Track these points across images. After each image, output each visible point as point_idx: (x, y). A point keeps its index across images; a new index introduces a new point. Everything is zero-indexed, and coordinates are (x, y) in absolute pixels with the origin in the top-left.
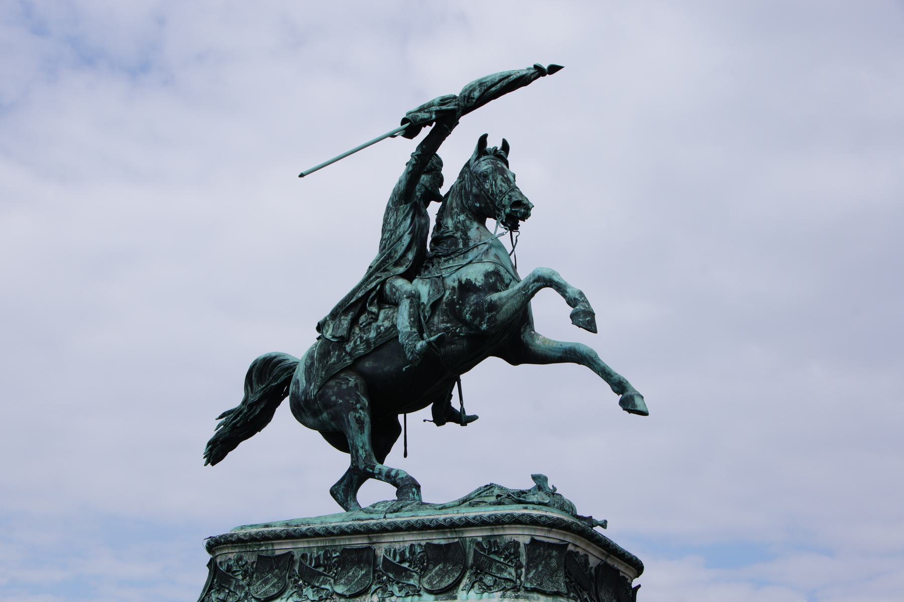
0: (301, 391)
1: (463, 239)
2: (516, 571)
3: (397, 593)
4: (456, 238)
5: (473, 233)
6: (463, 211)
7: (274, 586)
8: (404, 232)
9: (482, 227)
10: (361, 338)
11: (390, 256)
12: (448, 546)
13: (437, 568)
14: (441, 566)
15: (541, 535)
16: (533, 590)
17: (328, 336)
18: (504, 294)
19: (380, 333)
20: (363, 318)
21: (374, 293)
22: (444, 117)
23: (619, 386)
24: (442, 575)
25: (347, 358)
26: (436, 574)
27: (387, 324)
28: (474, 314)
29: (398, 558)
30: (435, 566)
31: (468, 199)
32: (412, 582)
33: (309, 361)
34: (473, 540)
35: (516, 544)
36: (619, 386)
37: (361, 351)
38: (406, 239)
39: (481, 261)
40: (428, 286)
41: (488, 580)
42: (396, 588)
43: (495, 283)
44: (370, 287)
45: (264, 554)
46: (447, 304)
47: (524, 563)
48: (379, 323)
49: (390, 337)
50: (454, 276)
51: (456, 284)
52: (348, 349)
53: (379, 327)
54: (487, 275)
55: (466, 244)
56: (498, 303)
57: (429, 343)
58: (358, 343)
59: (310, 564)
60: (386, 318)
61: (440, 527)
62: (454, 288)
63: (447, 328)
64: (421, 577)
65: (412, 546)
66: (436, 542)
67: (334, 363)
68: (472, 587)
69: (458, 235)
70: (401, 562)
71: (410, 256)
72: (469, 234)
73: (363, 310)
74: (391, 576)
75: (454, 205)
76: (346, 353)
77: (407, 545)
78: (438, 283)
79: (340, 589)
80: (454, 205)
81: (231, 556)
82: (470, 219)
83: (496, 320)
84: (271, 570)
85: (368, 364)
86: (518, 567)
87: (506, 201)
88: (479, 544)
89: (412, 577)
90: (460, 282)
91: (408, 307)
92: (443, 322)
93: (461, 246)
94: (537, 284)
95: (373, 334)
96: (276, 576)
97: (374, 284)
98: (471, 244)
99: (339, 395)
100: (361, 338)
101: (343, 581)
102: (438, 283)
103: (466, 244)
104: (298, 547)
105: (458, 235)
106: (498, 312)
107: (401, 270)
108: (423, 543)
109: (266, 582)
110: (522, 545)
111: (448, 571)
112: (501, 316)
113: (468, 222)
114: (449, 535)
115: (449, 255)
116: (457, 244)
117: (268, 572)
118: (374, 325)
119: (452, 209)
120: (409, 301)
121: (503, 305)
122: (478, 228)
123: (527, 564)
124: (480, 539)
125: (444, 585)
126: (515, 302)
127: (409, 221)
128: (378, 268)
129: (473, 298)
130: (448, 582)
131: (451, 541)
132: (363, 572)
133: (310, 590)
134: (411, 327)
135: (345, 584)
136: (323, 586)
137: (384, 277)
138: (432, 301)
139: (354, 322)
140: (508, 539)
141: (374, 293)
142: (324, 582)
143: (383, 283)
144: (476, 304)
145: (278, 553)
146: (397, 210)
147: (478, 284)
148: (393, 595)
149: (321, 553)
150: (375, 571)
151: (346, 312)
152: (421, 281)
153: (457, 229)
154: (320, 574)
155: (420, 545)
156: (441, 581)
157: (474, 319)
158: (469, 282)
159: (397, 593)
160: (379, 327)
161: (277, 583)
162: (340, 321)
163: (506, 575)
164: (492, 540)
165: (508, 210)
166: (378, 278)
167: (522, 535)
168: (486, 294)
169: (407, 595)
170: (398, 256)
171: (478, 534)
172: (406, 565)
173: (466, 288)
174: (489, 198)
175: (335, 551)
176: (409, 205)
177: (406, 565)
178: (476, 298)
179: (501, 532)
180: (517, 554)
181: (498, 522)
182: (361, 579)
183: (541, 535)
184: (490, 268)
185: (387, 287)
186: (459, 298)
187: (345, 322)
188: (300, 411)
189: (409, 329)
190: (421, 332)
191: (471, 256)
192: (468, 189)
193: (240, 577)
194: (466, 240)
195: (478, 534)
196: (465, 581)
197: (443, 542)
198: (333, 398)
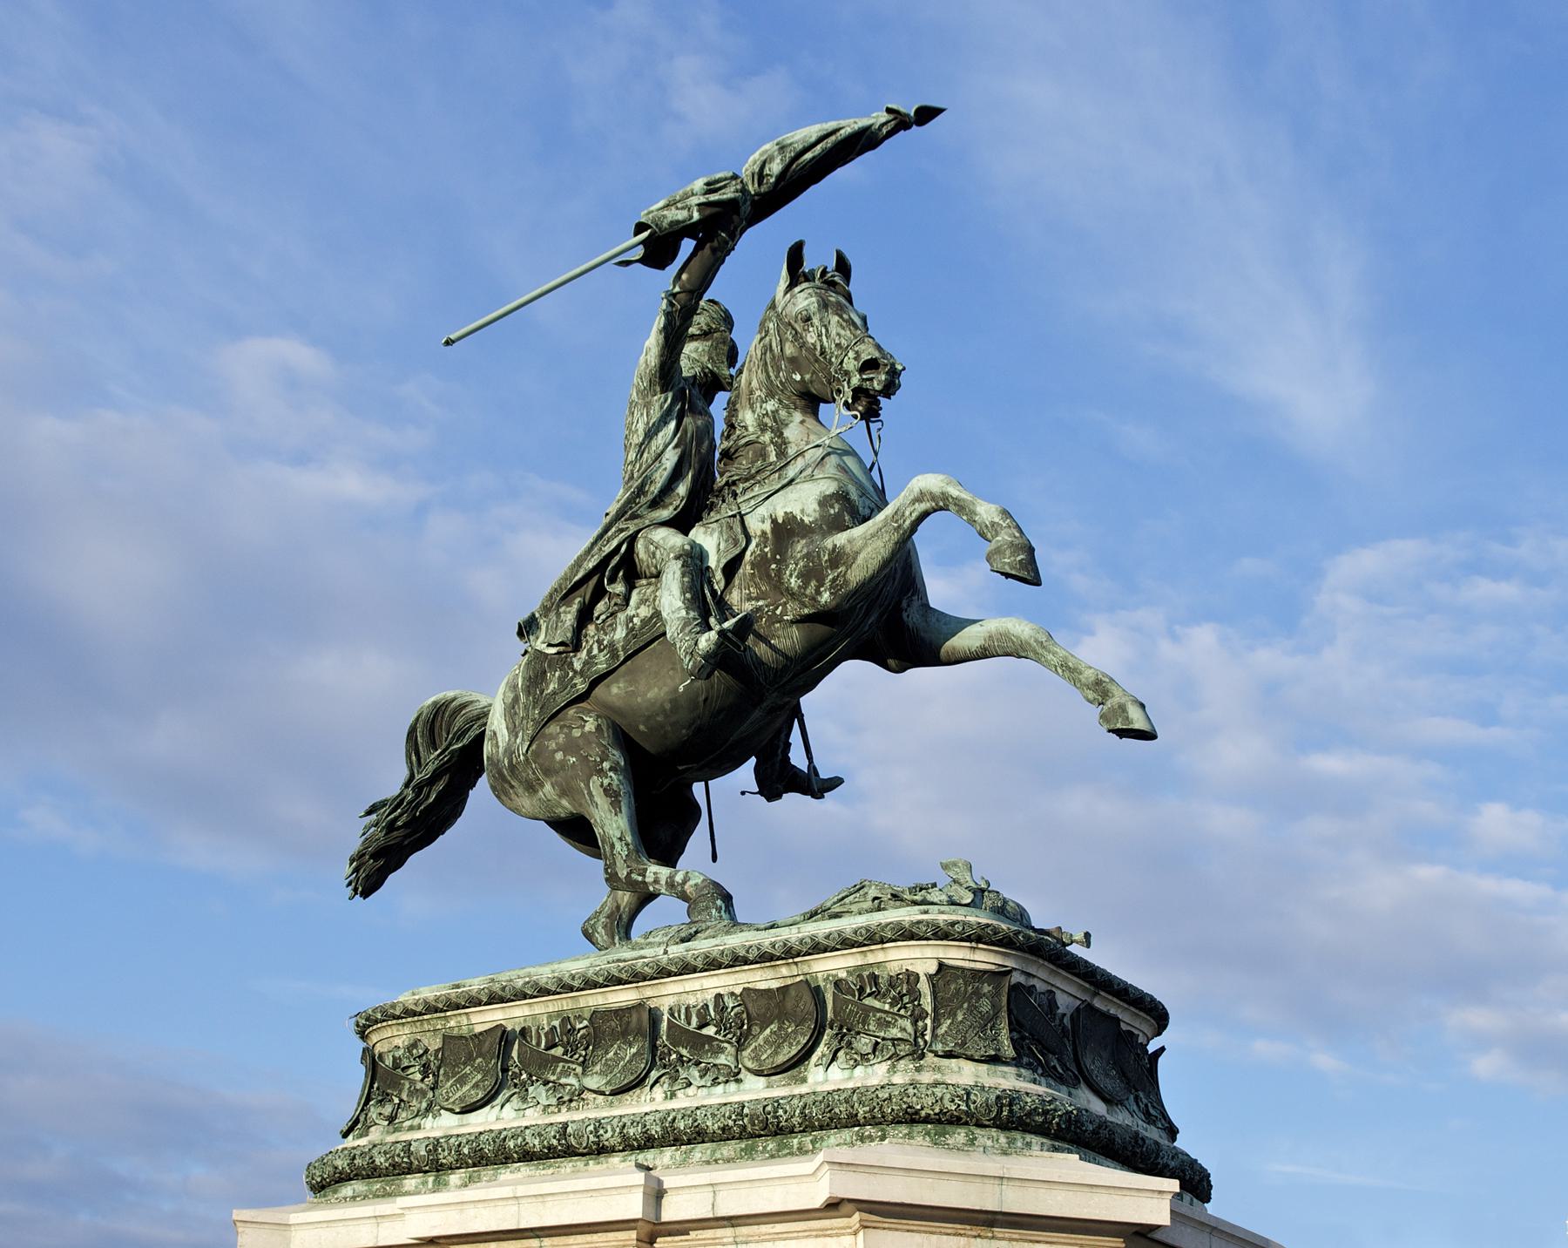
1: (775, 444)
2: (915, 1023)
3: (697, 1082)
4: (764, 446)
5: (793, 432)
6: (771, 394)
7: (476, 1086)
8: (666, 446)
9: (810, 422)
10: (600, 642)
11: (641, 491)
12: (784, 990)
13: (768, 1031)
14: (774, 1027)
15: (958, 955)
16: (949, 1055)
17: (540, 645)
18: (858, 531)
19: (633, 629)
20: (600, 607)
21: (617, 558)
22: (721, 224)
24: (777, 1043)
25: (578, 680)
26: (766, 1041)
27: (645, 612)
28: (805, 576)
29: (694, 1021)
30: (763, 1029)
31: (779, 369)
32: (722, 1060)
33: (511, 695)
35: (912, 978)
38: (670, 458)
39: (811, 478)
40: (716, 535)
41: (864, 1044)
43: (838, 515)
44: (607, 549)
45: (455, 1032)
46: (753, 565)
47: (929, 1009)
48: (630, 611)
49: (650, 636)
50: (763, 510)
51: (767, 527)
52: (577, 666)
53: (630, 619)
54: (824, 502)
55: (781, 453)
56: (848, 550)
57: (721, 633)
58: (595, 651)
59: (538, 1044)
60: (643, 602)
61: (765, 958)
62: (764, 533)
63: (759, 609)
64: (740, 1047)
65: (719, 997)
66: (762, 986)
67: (554, 693)
68: (834, 1058)
70: (701, 1027)
71: (682, 489)
72: (787, 433)
73: (599, 593)
74: (684, 1052)
75: (755, 384)
76: (575, 672)
77: (709, 997)
80: (755, 384)
81: (398, 1042)
82: (787, 407)
83: (846, 582)
84: (470, 1059)
85: (614, 691)
86: (917, 1017)
87: (850, 364)
88: (838, 984)
89: (722, 1050)
90: (774, 521)
91: (678, 574)
92: (749, 599)
93: (773, 458)
94: (921, 507)
95: (620, 633)
96: (478, 1069)
97: (615, 543)
98: (791, 451)
99: (570, 747)
100: (600, 642)
101: (598, 1068)
103: (781, 453)
105: (767, 437)
106: (849, 567)
107: (665, 514)
108: (738, 991)
109: (462, 1081)
110: (923, 978)
111: (788, 1035)
112: (856, 574)
113: (783, 413)
115: (753, 477)
116: (763, 455)
117: (465, 1064)
118: (621, 616)
119: (751, 393)
120: (680, 563)
121: (857, 553)
122: (802, 422)
123: (935, 1010)
124: (843, 975)
125: (781, 1059)
126: (880, 543)
127: (673, 425)
128: (620, 515)
129: (800, 547)
130: (788, 1052)
131: (789, 982)
132: (634, 1050)
133: (542, 1089)
134: (688, 609)
135: (602, 1073)
136: (563, 1081)
137: (632, 529)
138: (724, 561)
139: (585, 616)
140: (894, 968)
141: (617, 558)
142: (565, 1073)
143: (632, 540)
144: (808, 556)
145: (478, 1029)
146: (647, 405)
147: (806, 520)
148: (690, 1084)
149: (556, 1023)
150: (654, 1048)
151: (567, 597)
152: (702, 529)
153: (763, 428)
154: (557, 1060)
155: (732, 994)
156: (776, 1053)
157: (806, 584)
158: (790, 518)
159: (697, 1082)
160: (630, 619)
161: (482, 1080)
162: (558, 615)
164: (866, 974)
165: (855, 381)
166: (622, 530)
167: (920, 959)
168: (825, 535)
169: (715, 1082)
170: (655, 489)
171: (837, 964)
172: (710, 1031)
173: (786, 531)
174: (817, 360)
175: (580, 1018)
176: (670, 395)
177: (710, 1031)
178: (807, 545)
179: (880, 957)
181: (873, 938)
182: (630, 1061)
183: (958, 955)
184: (830, 488)
185: (640, 546)
186: (775, 552)
187: (569, 616)
188: (501, 790)
189: (683, 613)
190: (705, 614)
191: (791, 472)
192: (776, 350)
193: (418, 1077)
194: (782, 446)
195: (837, 964)
196: (822, 1049)
197: (774, 985)
198: (559, 756)
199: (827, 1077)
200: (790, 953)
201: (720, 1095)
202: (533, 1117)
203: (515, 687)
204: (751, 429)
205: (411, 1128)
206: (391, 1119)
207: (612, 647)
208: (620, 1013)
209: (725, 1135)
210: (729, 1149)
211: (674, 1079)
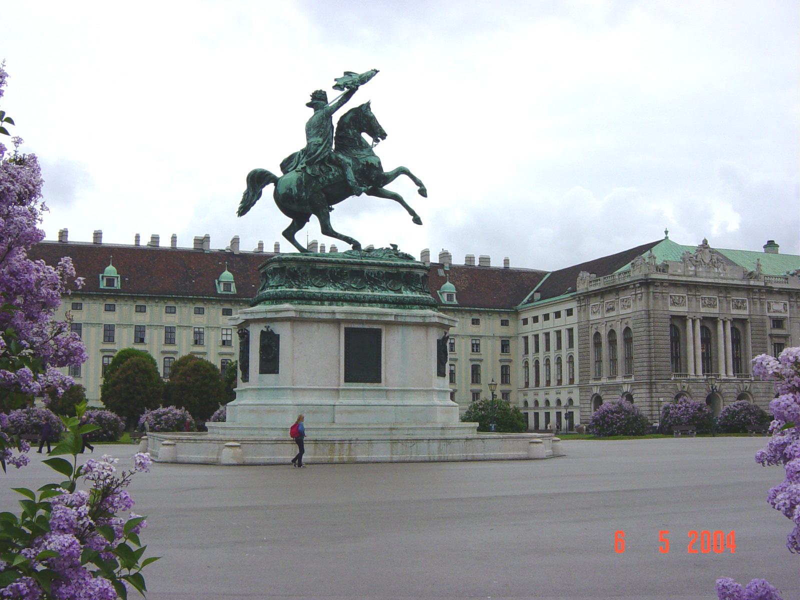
0: (293, 193)
10: (326, 178)
13: (391, 281)
23: (412, 212)
30: (390, 280)
32: (382, 285)
33: (299, 182)
34: (402, 272)
35: (418, 275)
36: (412, 212)
37: (327, 183)
42: (376, 287)
51: (365, 163)
62: (363, 164)
69: (356, 139)
76: (320, 183)
78: (355, 160)
79: (353, 285)
93: (358, 144)
100: (326, 178)
102: (355, 160)
104: (329, 266)
108: (384, 272)
109: (317, 279)
114: (393, 270)
125: (396, 288)
148: (376, 289)
156: (394, 286)
158: (372, 164)
163: (418, 286)
169: (383, 290)
171: (405, 270)
180: (419, 279)
195: (405, 270)
196: (403, 287)
199: (407, 294)
200: (397, 266)
201: (384, 293)
202: (338, 291)
203: (301, 181)
204: (351, 135)
205: (305, 288)
206: (299, 285)
207: (329, 180)
208: (356, 271)
209: (393, 303)
210: (392, 306)
211: (372, 288)
